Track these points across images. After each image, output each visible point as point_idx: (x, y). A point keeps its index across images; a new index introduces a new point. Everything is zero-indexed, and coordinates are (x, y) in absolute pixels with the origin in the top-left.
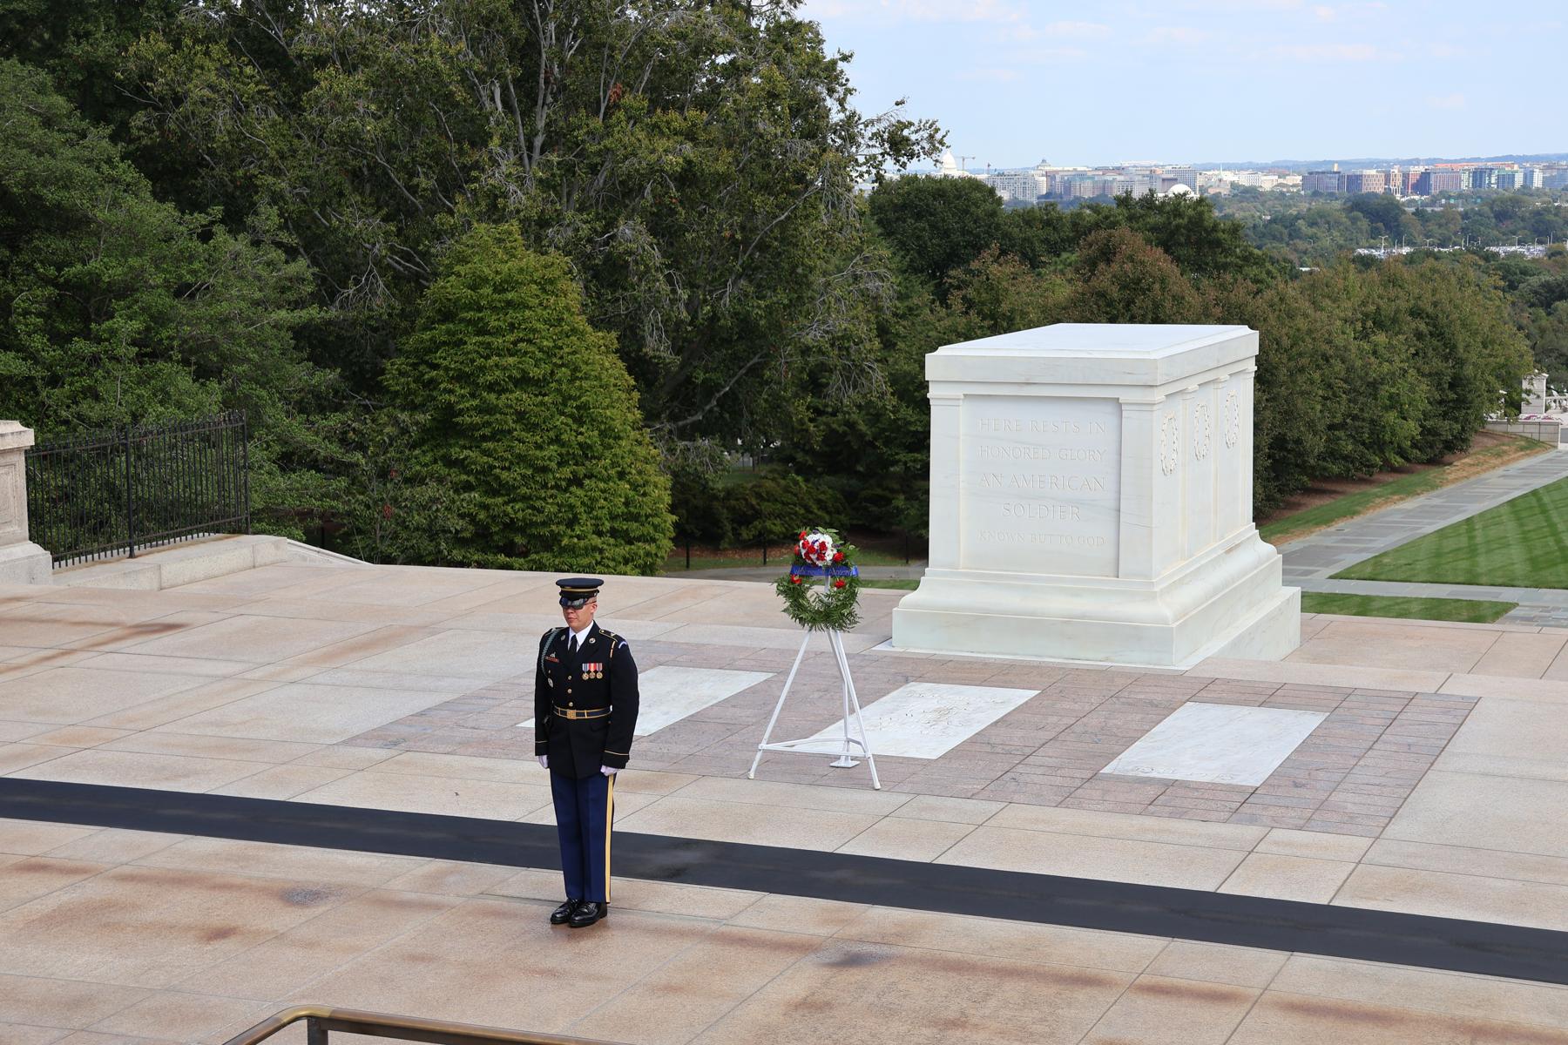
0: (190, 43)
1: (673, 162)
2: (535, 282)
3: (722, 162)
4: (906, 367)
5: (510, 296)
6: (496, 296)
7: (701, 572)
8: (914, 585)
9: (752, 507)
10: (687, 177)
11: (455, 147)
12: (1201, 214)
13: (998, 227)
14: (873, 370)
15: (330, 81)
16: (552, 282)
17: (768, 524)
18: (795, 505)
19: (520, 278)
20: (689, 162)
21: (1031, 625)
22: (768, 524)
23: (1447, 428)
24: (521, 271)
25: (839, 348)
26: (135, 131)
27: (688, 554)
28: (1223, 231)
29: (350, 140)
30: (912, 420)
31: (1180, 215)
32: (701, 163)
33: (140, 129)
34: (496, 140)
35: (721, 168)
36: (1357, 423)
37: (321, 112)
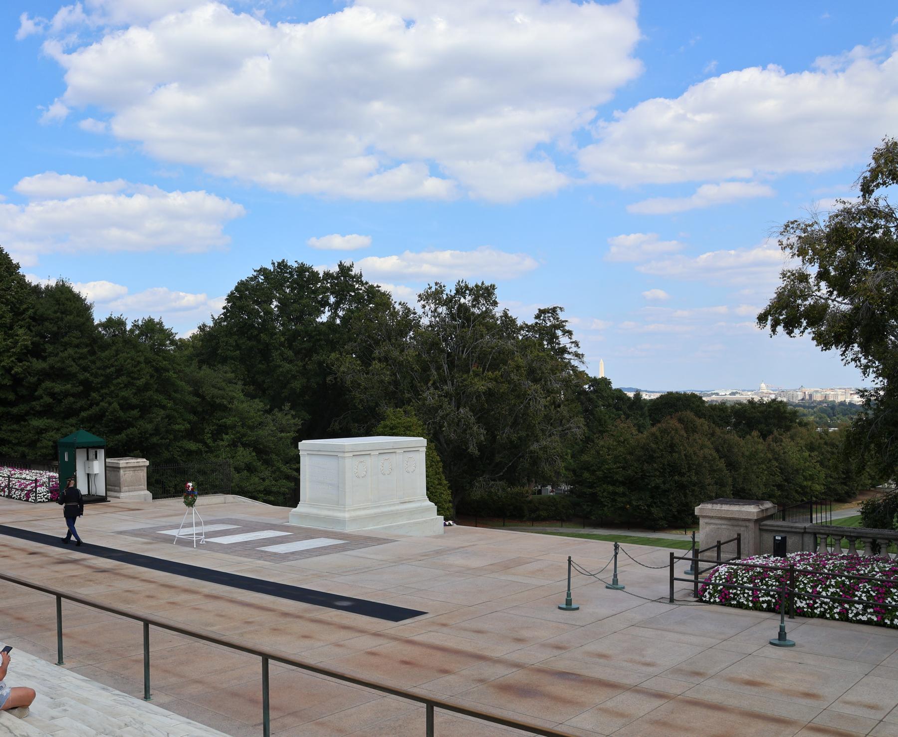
0: (345, 354)
1: (482, 389)
2: (404, 427)
3: (504, 387)
4: (587, 459)
5: (394, 431)
6: (390, 431)
7: (510, 528)
8: (296, 507)
9: (536, 507)
10: (490, 393)
11: (419, 384)
12: (779, 407)
13: (700, 411)
14: (557, 459)
15: (376, 365)
16: (410, 427)
17: (541, 513)
18: (552, 506)
19: (398, 425)
20: (489, 389)
21: (317, 518)
22: (541, 513)
23: (841, 489)
24: (399, 423)
25: (544, 451)
26: (327, 381)
27: (504, 522)
28: (788, 413)
29: (382, 381)
30: (588, 477)
31: (771, 407)
32: (494, 389)
33: (329, 381)
34: (431, 382)
35: (501, 391)
36: (790, 485)
37: (373, 374)
